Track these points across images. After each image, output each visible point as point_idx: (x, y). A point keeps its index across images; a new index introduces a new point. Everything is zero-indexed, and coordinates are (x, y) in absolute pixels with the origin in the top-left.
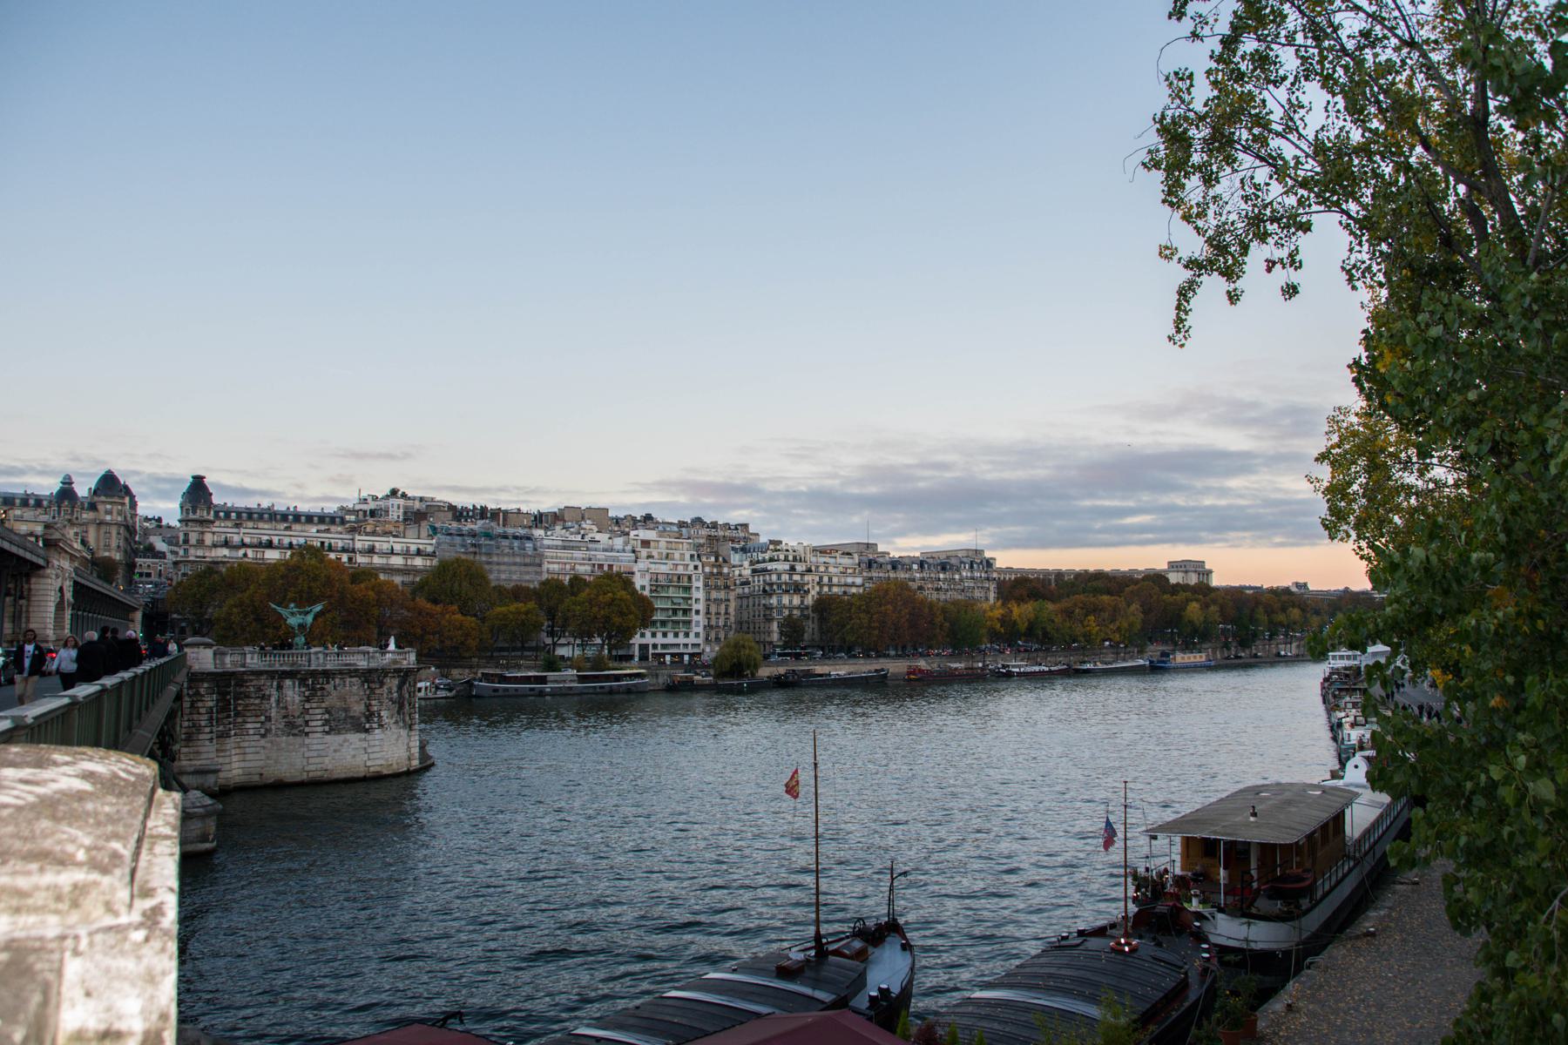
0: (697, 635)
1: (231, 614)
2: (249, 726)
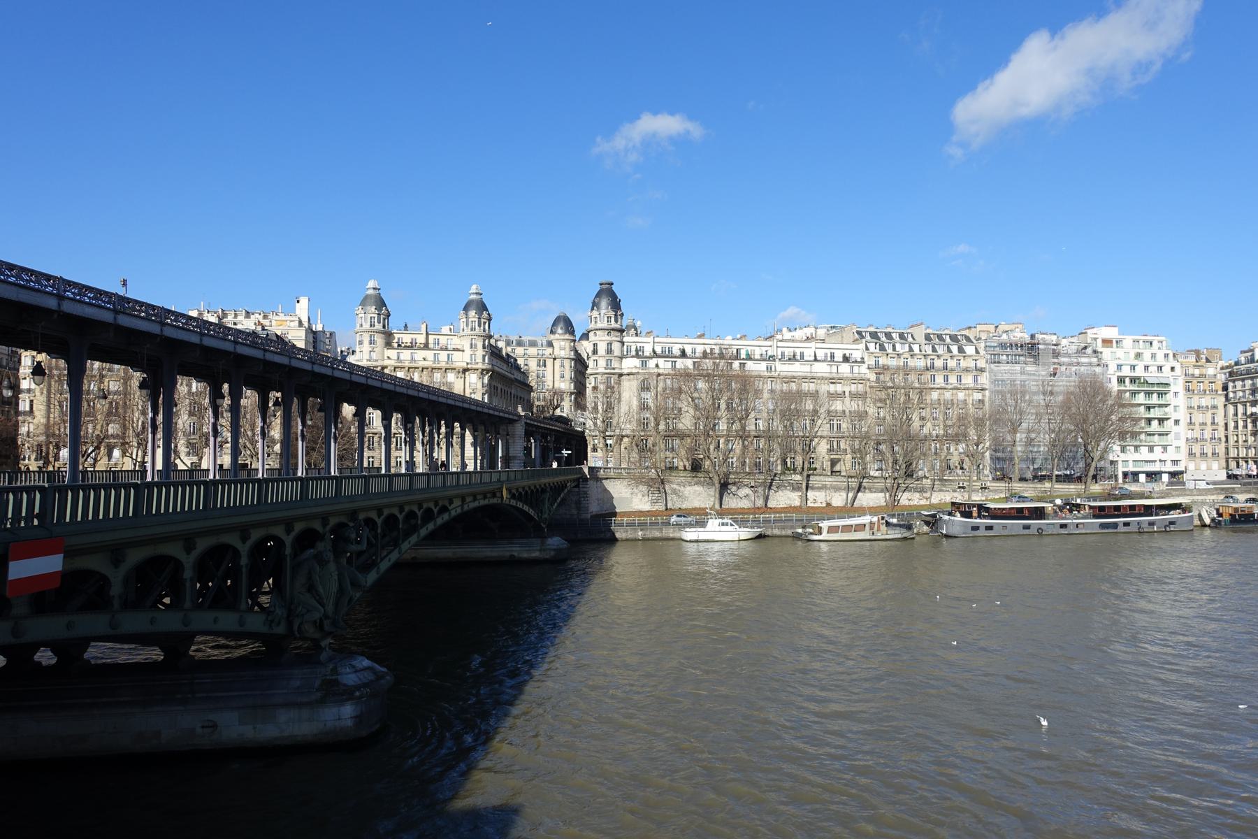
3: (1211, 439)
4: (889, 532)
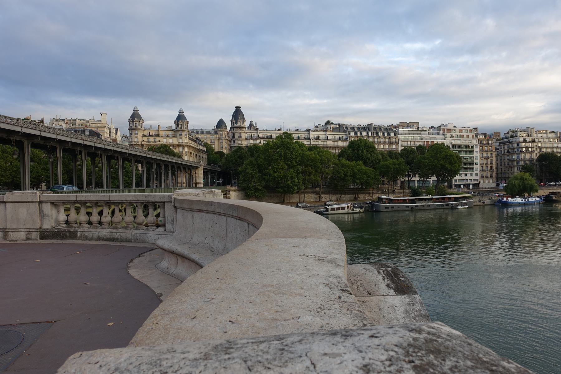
0: (477, 174)
1: (246, 169)
3: (490, 170)
4: (354, 210)
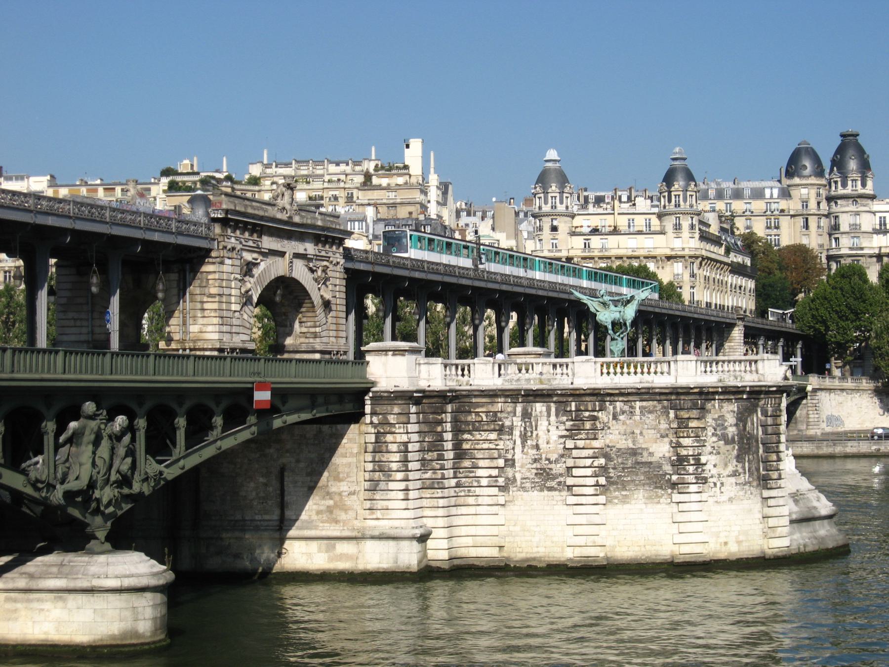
2: (480, 472)
